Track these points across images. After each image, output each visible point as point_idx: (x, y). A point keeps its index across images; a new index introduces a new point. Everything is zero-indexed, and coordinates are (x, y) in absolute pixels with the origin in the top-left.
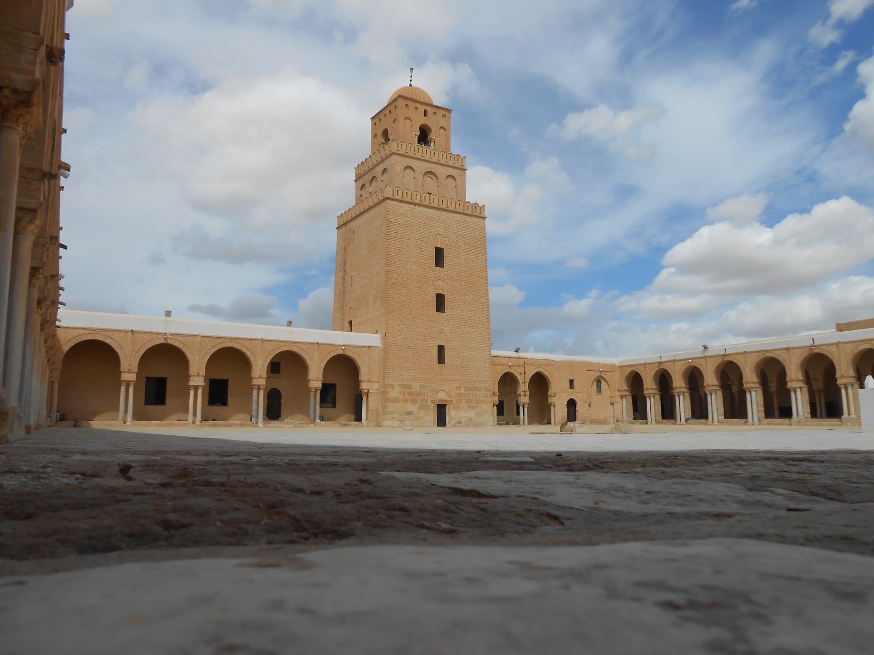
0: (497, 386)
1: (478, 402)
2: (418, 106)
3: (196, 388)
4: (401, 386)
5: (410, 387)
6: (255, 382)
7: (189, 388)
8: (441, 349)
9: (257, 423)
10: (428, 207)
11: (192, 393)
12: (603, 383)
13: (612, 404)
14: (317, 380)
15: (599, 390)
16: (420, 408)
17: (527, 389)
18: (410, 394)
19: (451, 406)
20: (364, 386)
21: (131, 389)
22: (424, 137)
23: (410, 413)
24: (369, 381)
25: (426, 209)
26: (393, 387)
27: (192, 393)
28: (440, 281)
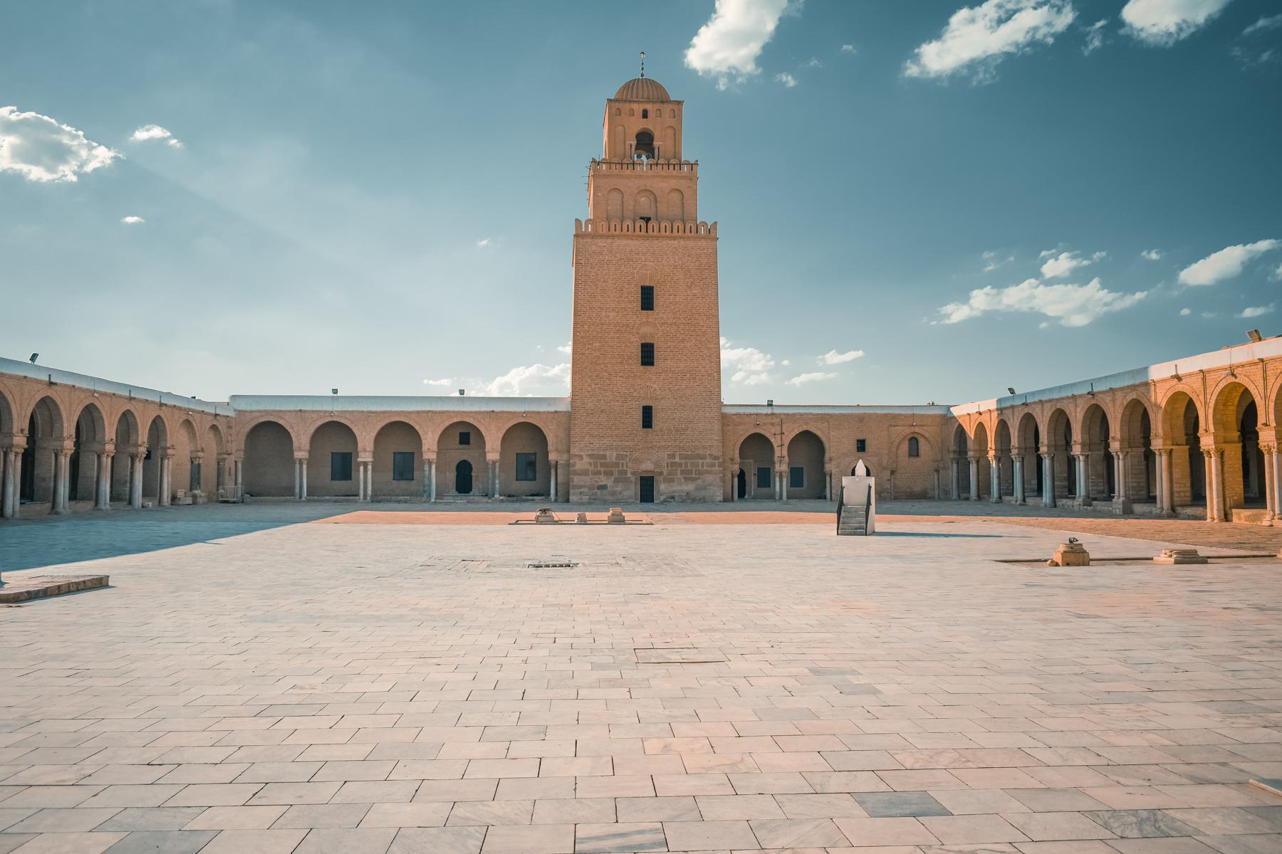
1: (700, 473)
2: (635, 106)
3: (365, 464)
5: (604, 457)
6: (426, 456)
7: (359, 464)
11: (362, 468)
12: (922, 442)
13: (937, 471)
15: (914, 451)
16: (617, 481)
17: (785, 453)
18: (602, 465)
19: (661, 478)
21: (305, 466)
22: (645, 142)
24: (557, 450)
26: (581, 457)
27: (362, 468)
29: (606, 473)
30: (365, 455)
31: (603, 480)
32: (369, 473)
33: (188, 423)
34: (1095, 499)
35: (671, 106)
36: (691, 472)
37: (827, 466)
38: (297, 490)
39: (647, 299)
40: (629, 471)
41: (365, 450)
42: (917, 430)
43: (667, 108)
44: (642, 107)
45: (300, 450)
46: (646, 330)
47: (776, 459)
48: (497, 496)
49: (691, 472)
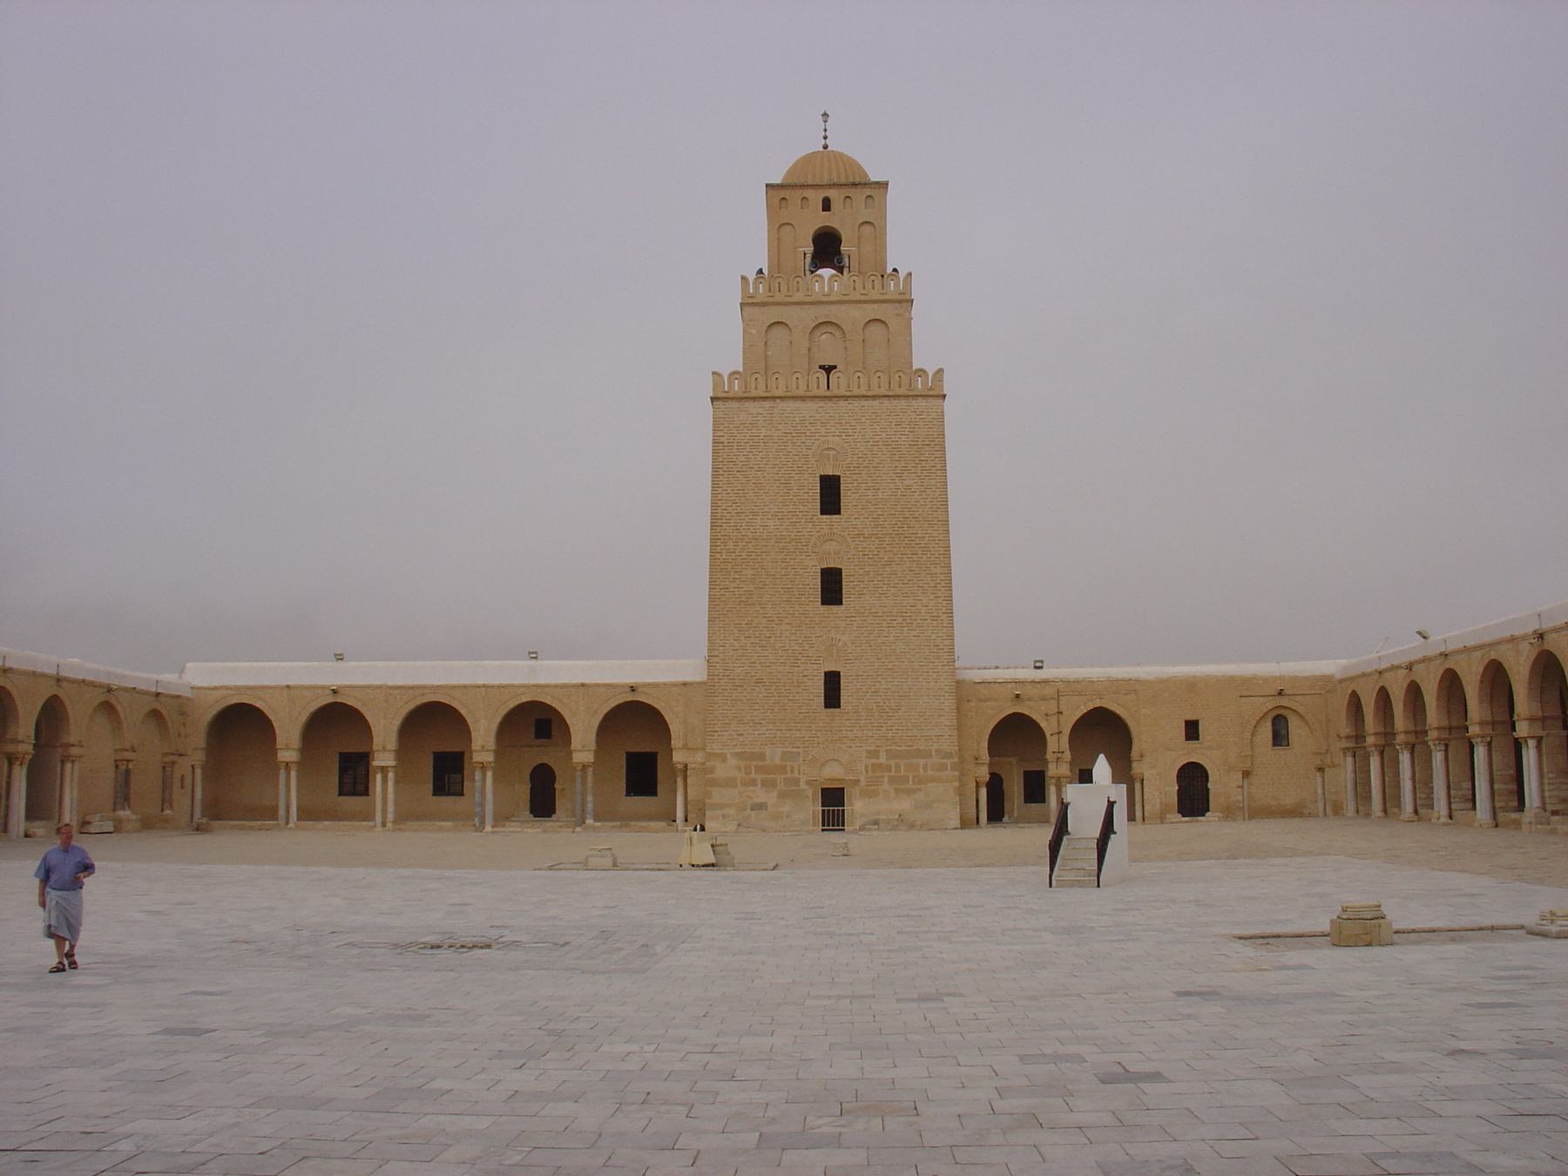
2: (808, 193)
3: (384, 770)
4: (740, 756)
5: (762, 756)
6: (477, 758)
9: (483, 823)
10: (803, 398)
11: (379, 777)
13: (1321, 770)
15: (1280, 736)
16: (783, 796)
17: (1065, 745)
18: (760, 769)
19: (856, 791)
20: (678, 757)
21: (293, 774)
22: (827, 249)
23: (760, 807)
24: (685, 747)
25: (799, 404)
26: (723, 758)
27: (379, 777)
28: (832, 540)
29: (765, 784)
30: (384, 757)
31: (760, 796)
32: (390, 784)
33: (108, 708)
34: (1555, 813)
35: (868, 192)
36: (905, 779)
37: (1134, 765)
38: (282, 812)
39: (830, 495)
41: (384, 749)
42: (1285, 702)
43: (859, 196)
44: (822, 194)
45: (287, 748)
47: (1049, 756)
48: (590, 821)
49: (906, 779)
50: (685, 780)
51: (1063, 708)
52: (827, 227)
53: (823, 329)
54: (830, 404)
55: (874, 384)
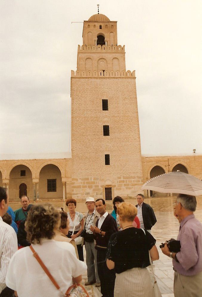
0: (149, 175)
2: (96, 24)
5: (88, 179)
8: (107, 158)
10: (97, 78)
14: (36, 178)
18: (88, 183)
19: (115, 188)
20: (64, 180)
22: (101, 40)
24: (66, 177)
25: (95, 80)
26: (77, 180)
28: (106, 118)
39: (105, 105)
40: (99, 186)
46: (106, 119)
49: (128, 185)
50: (66, 187)
51: (170, 164)
52: (100, 34)
53: (101, 60)
54: (104, 80)
55: (117, 74)
